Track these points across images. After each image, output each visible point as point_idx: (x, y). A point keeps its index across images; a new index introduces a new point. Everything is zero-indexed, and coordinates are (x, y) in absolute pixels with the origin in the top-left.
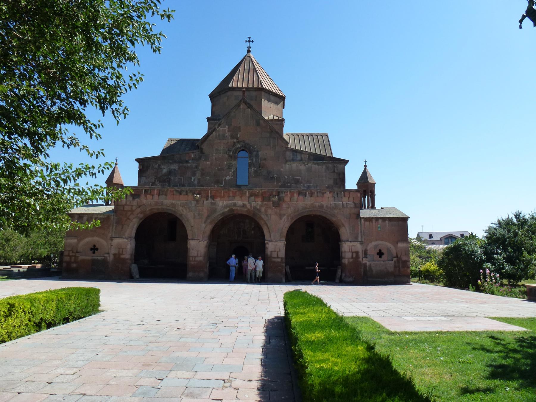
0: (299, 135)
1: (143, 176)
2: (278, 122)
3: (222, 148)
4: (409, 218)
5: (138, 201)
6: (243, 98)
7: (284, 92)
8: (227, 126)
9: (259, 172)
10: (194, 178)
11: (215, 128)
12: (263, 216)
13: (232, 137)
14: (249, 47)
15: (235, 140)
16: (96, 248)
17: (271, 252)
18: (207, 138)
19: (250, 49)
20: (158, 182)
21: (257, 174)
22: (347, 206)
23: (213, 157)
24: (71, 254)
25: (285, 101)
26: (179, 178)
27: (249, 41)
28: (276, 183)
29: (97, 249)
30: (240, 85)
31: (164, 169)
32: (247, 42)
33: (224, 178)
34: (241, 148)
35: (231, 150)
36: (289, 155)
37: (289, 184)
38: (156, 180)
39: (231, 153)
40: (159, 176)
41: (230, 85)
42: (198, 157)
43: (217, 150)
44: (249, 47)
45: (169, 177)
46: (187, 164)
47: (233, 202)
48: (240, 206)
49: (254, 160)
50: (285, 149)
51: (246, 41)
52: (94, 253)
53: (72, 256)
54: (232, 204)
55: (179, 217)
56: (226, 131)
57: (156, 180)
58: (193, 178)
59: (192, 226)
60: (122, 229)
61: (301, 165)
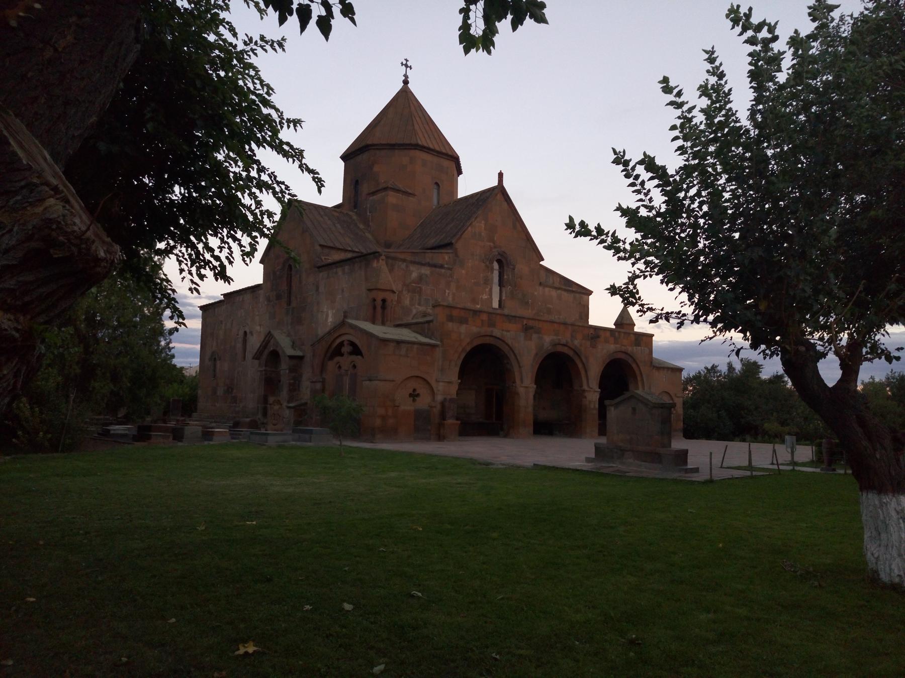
4: (684, 369)
8: (483, 222)
12: (584, 359)
14: (406, 76)
15: (492, 244)
19: (408, 79)
28: (530, 311)
32: (404, 66)
37: (542, 314)
39: (488, 263)
44: (406, 76)
47: (559, 337)
48: (564, 345)
51: (402, 64)
52: (414, 401)
56: (483, 229)
57: (404, 288)
58: (447, 291)
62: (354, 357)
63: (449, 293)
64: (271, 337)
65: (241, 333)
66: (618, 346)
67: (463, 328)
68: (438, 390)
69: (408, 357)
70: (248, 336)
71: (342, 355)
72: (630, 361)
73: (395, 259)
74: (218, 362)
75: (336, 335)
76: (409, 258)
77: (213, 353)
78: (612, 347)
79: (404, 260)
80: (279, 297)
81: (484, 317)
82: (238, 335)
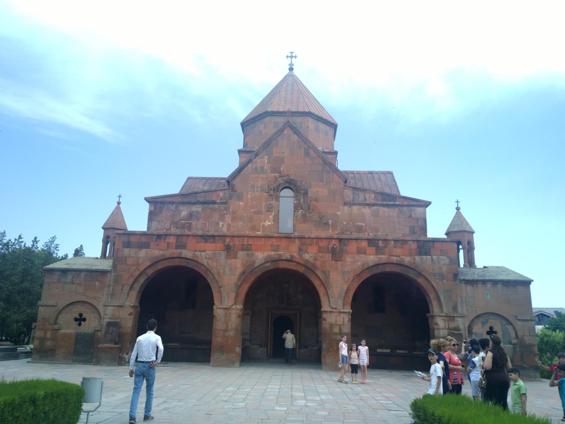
0: (355, 173)
1: (154, 221)
2: (329, 156)
3: (259, 185)
5: (147, 252)
6: (288, 122)
7: (337, 119)
8: (266, 157)
9: (308, 215)
10: (222, 223)
11: (251, 158)
13: (274, 170)
15: (277, 175)
16: (82, 317)
17: (331, 325)
18: (241, 171)
19: (293, 66)
21: (305, 219)
22: (439, 262)
23: (248, 196)
25: (337, 131)
26: (203, 223)
27: (292, 57)
28: (330, 231)
29: (84, 320)
30: (281, 109)
31: (183, 212)
32: (289, 58)
33: (262, 224)
34: (284, 185)
35: (271, 187)
36: (349, 194)
37: (348, 233)
38: (172, 226)
39: (272, 192)
40: (175, 220)
41: (269, 110)
42: (228, 195)
43: (253, 187)
45: (190, 221)
46: (214, 205)
47: (277, 253)
48: (287, 260)
49: (302, 200)
50: (342, 186)
51: (288, 57)
52: (80, 325)
54: (277, 256)
55: (202, 273)
56: (266, 163)
57: (172, 226)
58: (220, 223)
59: (220, 285)
61: (364, 208)
63: (223, 225)
66: (383, 256)
67: (143, 253)
68: (105, 314)
69: (74, 284)
72: (412, 275)
78: (372, 259)
79: (173, 203)
81: (172, 240)
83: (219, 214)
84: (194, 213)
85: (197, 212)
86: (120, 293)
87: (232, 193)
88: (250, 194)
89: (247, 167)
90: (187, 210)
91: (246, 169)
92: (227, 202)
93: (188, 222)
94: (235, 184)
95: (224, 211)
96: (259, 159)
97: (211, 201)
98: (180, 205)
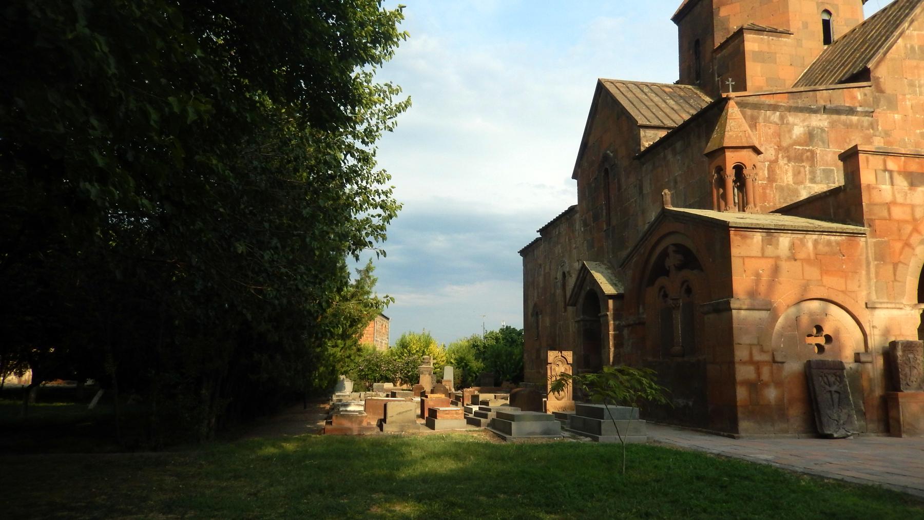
11: (904, 28)
20: (785, 161)
24: (758, 357)
31: (795, 127)
40: (785, 144)
42: (871, 99)
45: (811, 147)
46: (850, 117)
53: (765, 363)
57: (780, 156)
60: (895, 275)
62: (687, 273)
64: (586, 271)
65: (559, 276)
68: (873, 327)
69: (795, 260)
70: (567, 278)
71: (666, 273)
73: (757, 106)
74: (540, 316)
75: (654, 239)
76: (783, 101)
77: (535, 305)
79: (774, 108)
80: (596, 218)
82: (556, 278)
83: (862, 134)
84: (815, 132)
85: (820, 129)
86: (893, 281)
87: (877, 94)
88: (909, 100)
89: (896, 44)
90: (801, 124)
91: (894, 47)
92: (873, 112)
93: (807, 148)
94: (880, 76)
95: (869, 130)
96: (912, 30)
97: (847, 109)
98: (788, 114)
